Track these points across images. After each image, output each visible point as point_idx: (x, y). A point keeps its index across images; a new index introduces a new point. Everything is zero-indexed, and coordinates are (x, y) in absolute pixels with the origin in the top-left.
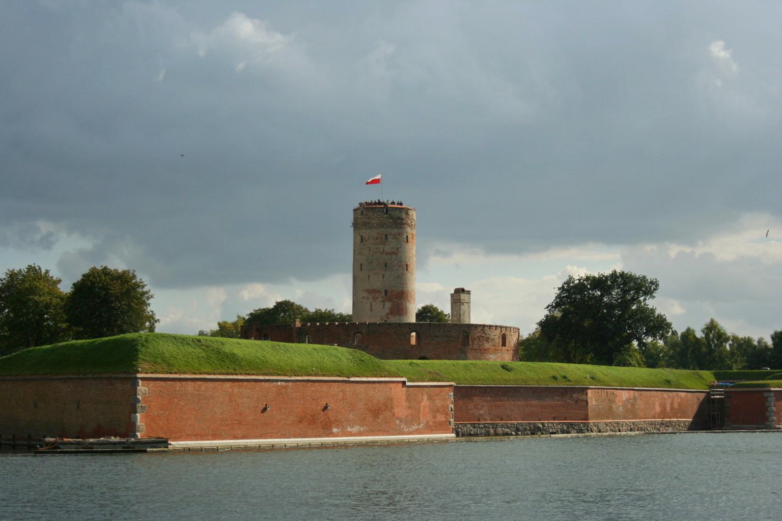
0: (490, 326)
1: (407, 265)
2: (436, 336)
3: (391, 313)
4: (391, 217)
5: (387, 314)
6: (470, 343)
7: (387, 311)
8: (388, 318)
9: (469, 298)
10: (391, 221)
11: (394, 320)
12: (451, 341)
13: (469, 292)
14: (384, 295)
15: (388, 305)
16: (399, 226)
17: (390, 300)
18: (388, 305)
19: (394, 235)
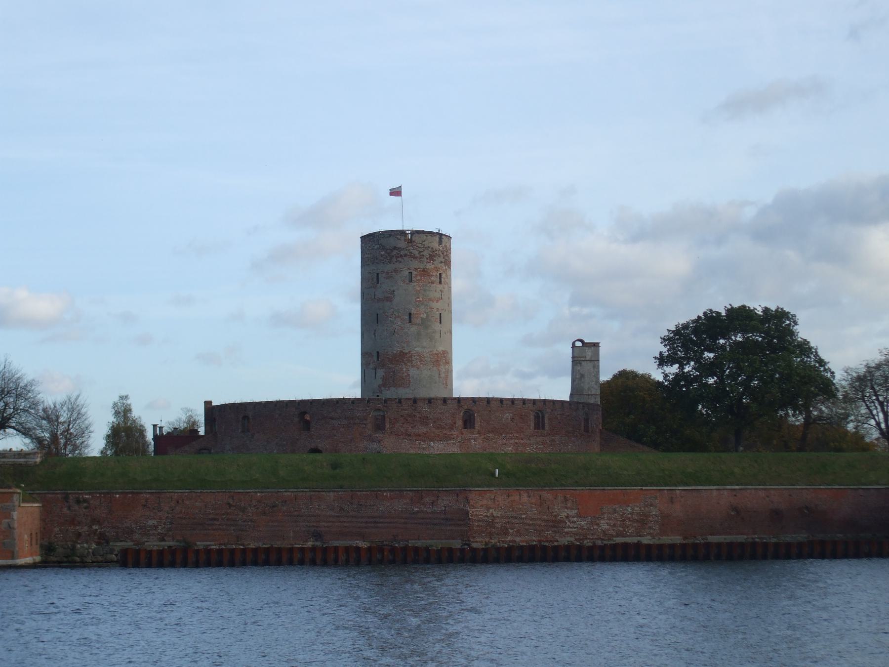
0: (430, 401)
1: (410, 314)
2: (332, 419)
3: (384, 385)
4: (383, 248)
5: (380, 386)
6: (388, 426)
7: (380, 382)
8: (381, 392)
9: (597, 354)
10: (383, 253)
11: (389, 393)
12: (354, 424)
13: (596, 345)
14: (375, 358)
15: (381, 373)
16: (394, 259)
17: (383, 366)
18: (381, 373)
19: (388, 273)
